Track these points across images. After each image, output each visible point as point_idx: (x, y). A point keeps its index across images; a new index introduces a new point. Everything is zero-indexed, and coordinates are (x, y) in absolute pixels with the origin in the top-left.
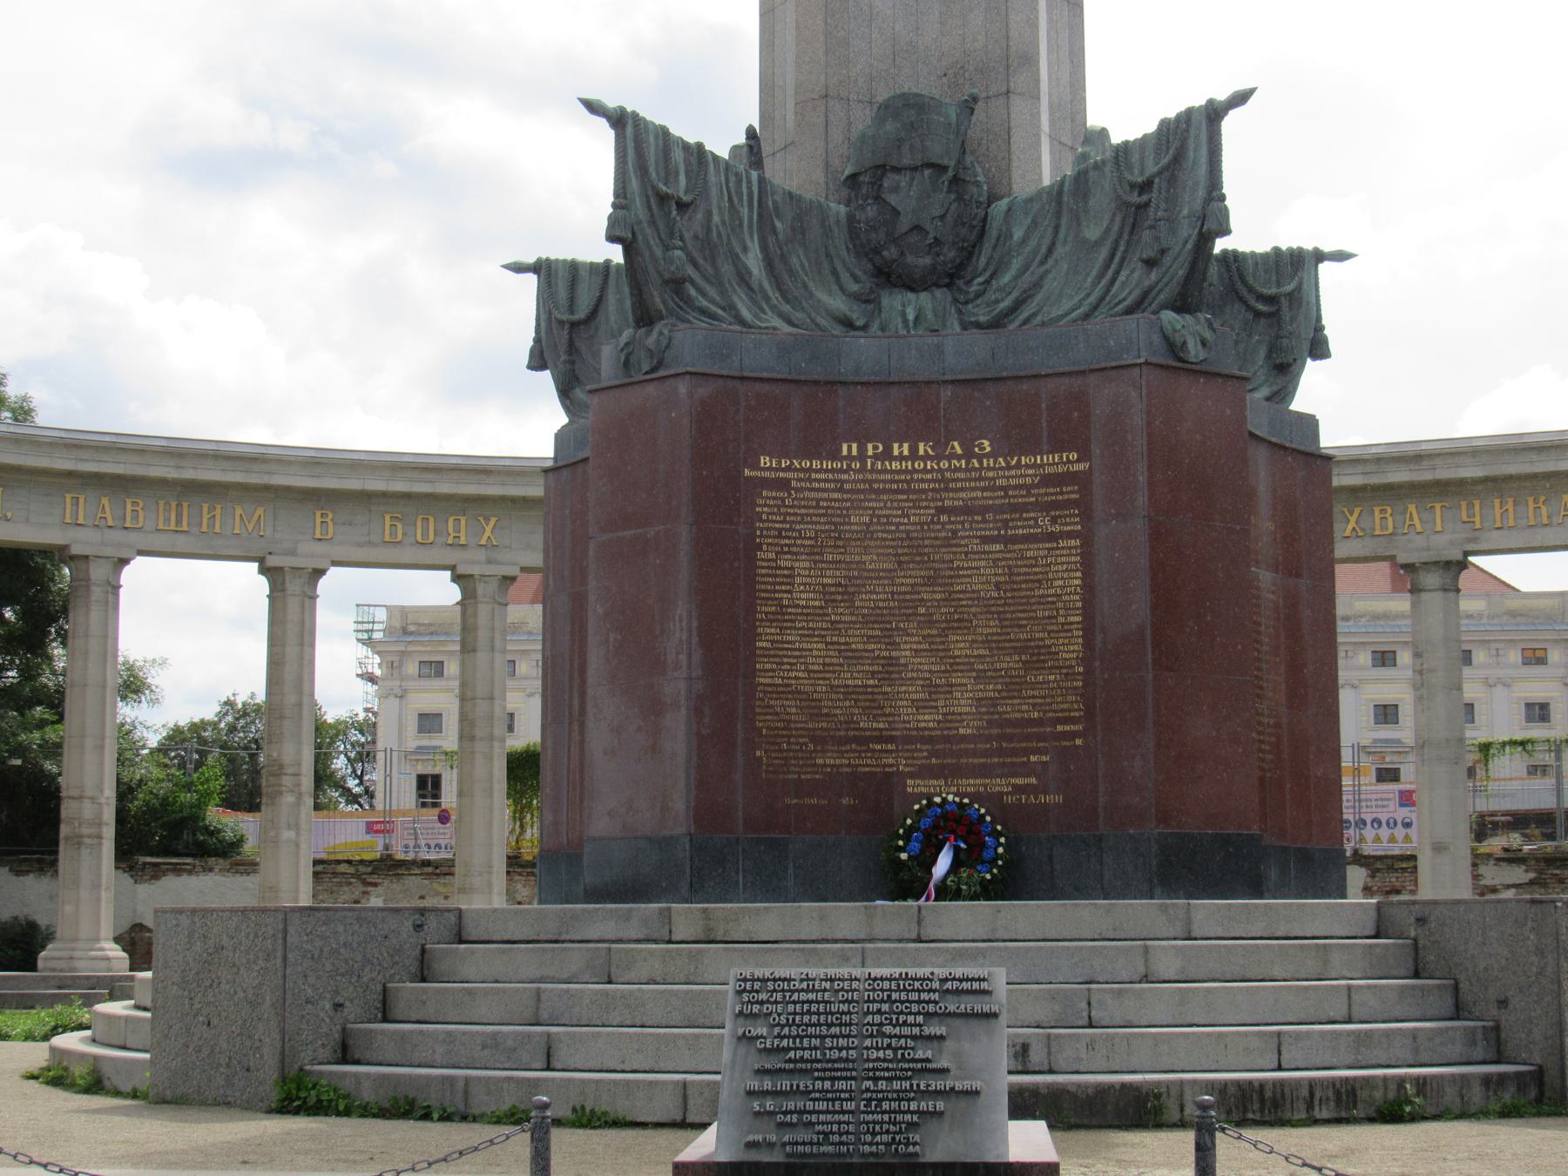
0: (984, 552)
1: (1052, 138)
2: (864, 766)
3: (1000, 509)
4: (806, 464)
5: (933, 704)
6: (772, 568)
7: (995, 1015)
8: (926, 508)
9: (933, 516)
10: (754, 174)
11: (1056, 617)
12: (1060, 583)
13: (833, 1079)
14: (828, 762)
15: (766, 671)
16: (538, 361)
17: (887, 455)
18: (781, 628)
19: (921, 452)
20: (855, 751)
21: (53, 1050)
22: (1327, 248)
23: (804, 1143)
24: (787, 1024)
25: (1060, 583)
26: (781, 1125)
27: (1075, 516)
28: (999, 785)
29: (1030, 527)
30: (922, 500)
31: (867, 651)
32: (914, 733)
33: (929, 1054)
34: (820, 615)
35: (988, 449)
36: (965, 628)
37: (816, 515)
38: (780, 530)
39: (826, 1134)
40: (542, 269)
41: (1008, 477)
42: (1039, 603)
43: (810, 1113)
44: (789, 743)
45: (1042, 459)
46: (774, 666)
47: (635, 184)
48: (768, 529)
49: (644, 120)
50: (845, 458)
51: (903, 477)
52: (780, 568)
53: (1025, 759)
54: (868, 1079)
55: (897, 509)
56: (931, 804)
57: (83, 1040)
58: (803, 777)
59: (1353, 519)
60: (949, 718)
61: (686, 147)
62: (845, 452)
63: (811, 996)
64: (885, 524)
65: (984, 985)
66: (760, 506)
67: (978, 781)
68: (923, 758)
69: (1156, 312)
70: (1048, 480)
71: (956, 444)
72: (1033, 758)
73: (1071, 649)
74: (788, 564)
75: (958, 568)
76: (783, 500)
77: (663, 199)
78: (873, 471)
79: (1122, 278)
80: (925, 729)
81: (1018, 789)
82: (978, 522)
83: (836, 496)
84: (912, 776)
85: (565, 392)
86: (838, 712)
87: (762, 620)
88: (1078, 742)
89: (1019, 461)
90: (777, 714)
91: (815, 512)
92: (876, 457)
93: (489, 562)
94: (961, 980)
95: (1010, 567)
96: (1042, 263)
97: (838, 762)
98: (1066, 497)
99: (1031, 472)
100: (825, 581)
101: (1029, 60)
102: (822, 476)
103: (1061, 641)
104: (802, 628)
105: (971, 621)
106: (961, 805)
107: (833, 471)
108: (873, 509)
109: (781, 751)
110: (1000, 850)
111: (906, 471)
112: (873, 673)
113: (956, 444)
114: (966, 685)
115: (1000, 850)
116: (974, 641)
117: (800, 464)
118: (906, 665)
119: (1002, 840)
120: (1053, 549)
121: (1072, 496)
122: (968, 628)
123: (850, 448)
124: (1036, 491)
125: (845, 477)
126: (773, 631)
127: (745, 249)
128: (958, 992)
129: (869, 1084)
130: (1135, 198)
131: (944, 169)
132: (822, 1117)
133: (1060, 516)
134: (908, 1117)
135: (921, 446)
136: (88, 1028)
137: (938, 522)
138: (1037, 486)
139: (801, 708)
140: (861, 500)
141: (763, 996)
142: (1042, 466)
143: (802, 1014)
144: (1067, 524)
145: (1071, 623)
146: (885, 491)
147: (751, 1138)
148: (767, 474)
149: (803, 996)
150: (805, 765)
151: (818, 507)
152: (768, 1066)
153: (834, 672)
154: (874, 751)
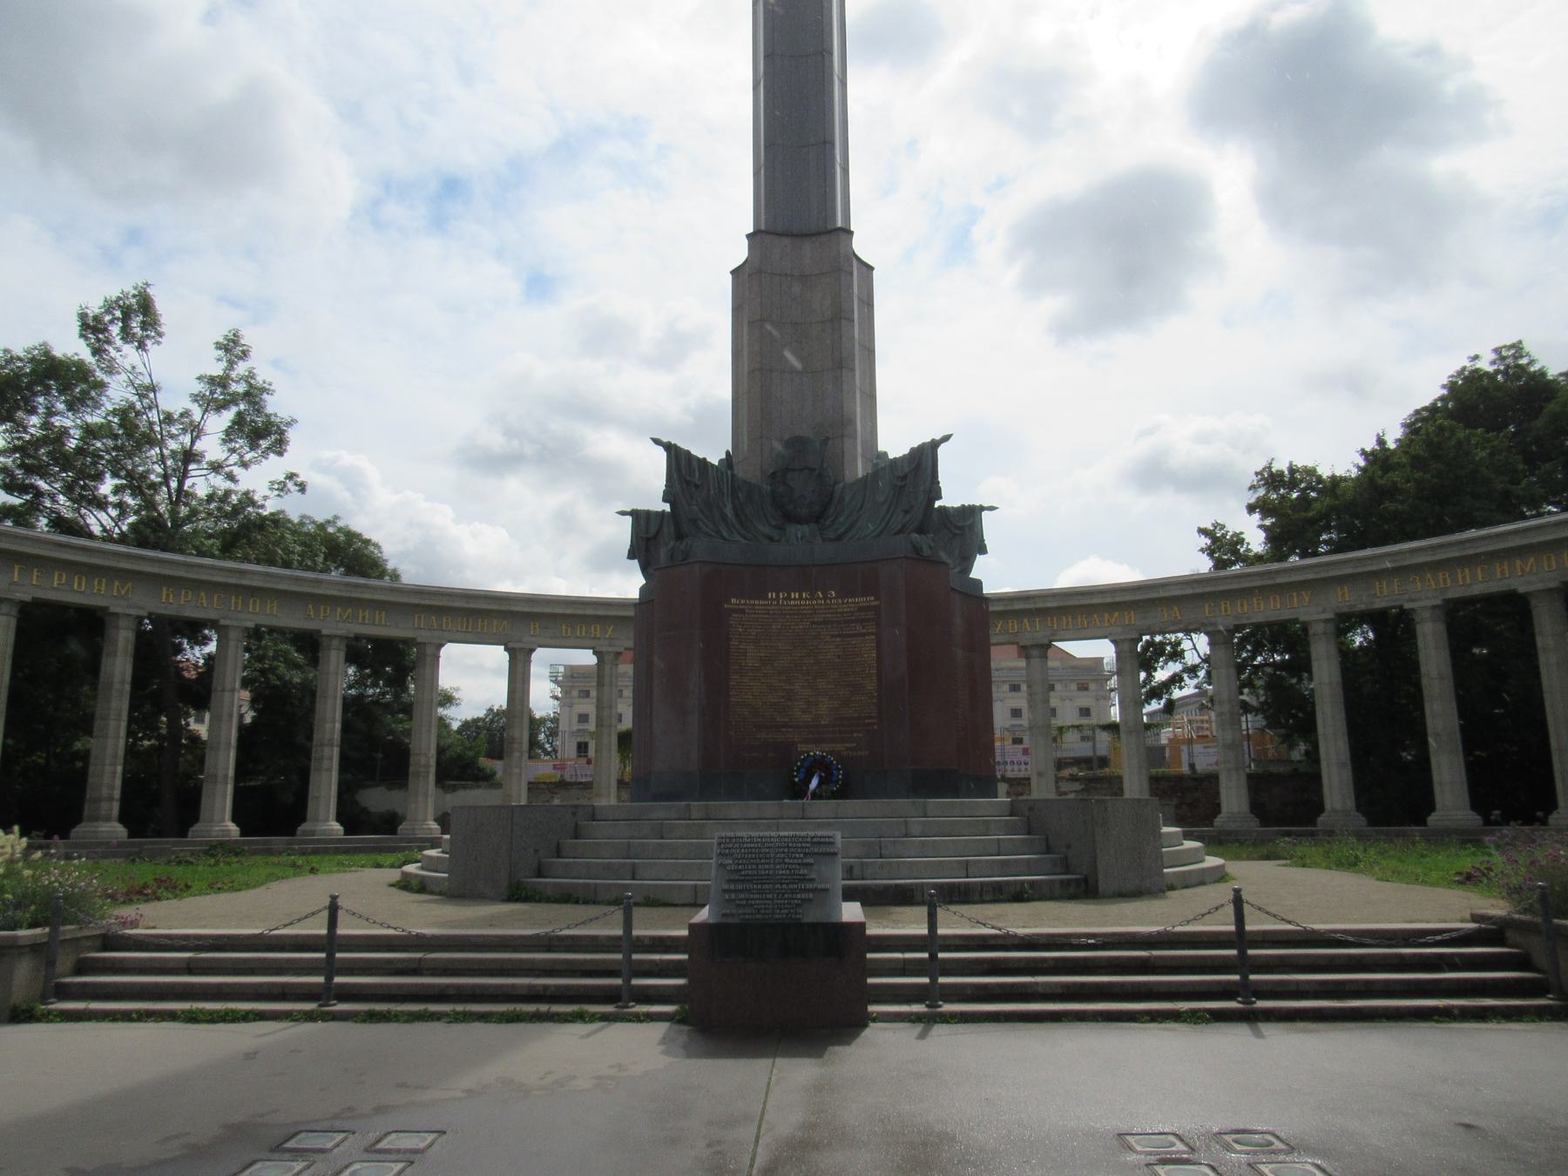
1: (863, 456)
4: (752, 602)
7: (835, 854)
10: (729, 472)
13: (762, 884)
16: (631, 555)
17: (789, 598)
19: (804, 596)
21: (405, 874)
22: (986, 506)
23: (749, 914)
24: (743, 859)
26: (738, 906)
28: (839, 747)
33: (806, 872)
39: (759, 910)
40: (635, 514)
43: (752, 899)
47: (675, 476)
49: (679, 447)
54: (778, 883)
56: (808, 755)
57: (417, 868)
59: (999, 626)
61: (699, 460)
63: (752, 845)
65: (831, 840)
69: (909, 534)
70: (861, 609)
71: (820, 593)
72: (855, 735)
73: (871, 686)
77: (688, 483)
79: (893, 519)
81: (848, 749)
83: (766, 616)
85: (644, 569)
88: (876, 727)
93: (610, 645)
94: (821, 837)
96: (858, 512)
101: (852, 422)
102: (758, 607)
106: (823, 756)
107: (764, 605)
110: (840, 777)
115: (840, 777)
119: (841, 772)
125: (769, 608)
127: (725, 505)
128: (820, 843)
129: (778, 886)
130: (899, 483)
131: (814, 470)
132: (757, 902)
134: (796, 901)
136: (419, 862)
141: (730, 845)
143: (748, 853)
147: (724, 911)
148: (734, 607)
149: (749, 845)
152: (732, 878)
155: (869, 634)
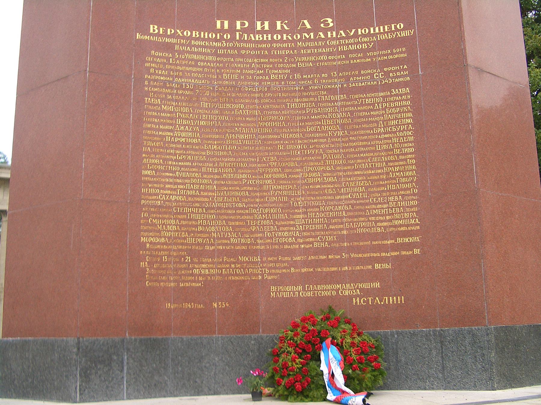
0: (331, 101)
3: (342, 68)
4: (188, 33)
5: (292, 222)
6: (157, 111)
8: (284, 68)
9: (288, 74)
11: (392, 150)
12: (395, 122)
15: (151, 195)
17: (252, 30)
18: (164, 160)
19: (279, 28)
20: (227, 263)
25: (395, 122)
27: (405, 70)
29: (367, 80)
30: (280, 63)
31: (237, 180)
32: (277, 247)
34: (196, 150)
35: (331, 25)
36: (317, 161)
37: (195, 72)
38: (165, 82)
41: (348, 45)
42: (378, 139)
44: (169, 256)
45: (374, 30)
46: (158, 191)
48: (155, 80)
50: (220, 31)
51: (264, 46)
52: (164, 111)
53: (370, 267)
55: (259, 69)
60: (305, 234)
62: (219, 26)
64: (250, 80)
66: (148, 62)
67: (329, 287)
68: (285, 268)
71: (306, 22)
72: (377, 266)
74: (171, 108)
75: (310, 114)
76: (168, 59)
78: (240, 41)
80: (285, 243)
81: (366, 293)
82: (325, 78)
83: (210, 58)
84: (275, 283)
86: (213, 229)
87: (147, 153)
88: (417, 251)
89: (356, 32)
90: (159, 231)
91: (194, 69)
92: (243, 30)
95: (352, 112)
98: (396, 56)
99: (365, 39)
100: (202, 123)
103: (397, 169)
104: (182, 161)
105: (321, 155)
107: (209, 40)
108: (242, 69)
111: (267, 42)
112: (241, 197)
113: (306, 22)
114: (318, 207)
116: (324, 171)
117: (183, 33)
118: (268, 191)
120: (387, 96)
121: (402, 55)
122: (319, 161)
123: (222, 24)
124: (371, 54)
126: (156, 161)
133: (391, 71)
135: (279, 23)
137: (293, 80)
138: (373, 49)
139: (181, 226)
140: (232, 62)
142: (375, 35)
144: (397, 77)
145: (406, 154)
146: (252, 57)
148: (155, 39)
151: (196, 66)
153: (208, 197)
154: (244, 262)
155: (398, 85)
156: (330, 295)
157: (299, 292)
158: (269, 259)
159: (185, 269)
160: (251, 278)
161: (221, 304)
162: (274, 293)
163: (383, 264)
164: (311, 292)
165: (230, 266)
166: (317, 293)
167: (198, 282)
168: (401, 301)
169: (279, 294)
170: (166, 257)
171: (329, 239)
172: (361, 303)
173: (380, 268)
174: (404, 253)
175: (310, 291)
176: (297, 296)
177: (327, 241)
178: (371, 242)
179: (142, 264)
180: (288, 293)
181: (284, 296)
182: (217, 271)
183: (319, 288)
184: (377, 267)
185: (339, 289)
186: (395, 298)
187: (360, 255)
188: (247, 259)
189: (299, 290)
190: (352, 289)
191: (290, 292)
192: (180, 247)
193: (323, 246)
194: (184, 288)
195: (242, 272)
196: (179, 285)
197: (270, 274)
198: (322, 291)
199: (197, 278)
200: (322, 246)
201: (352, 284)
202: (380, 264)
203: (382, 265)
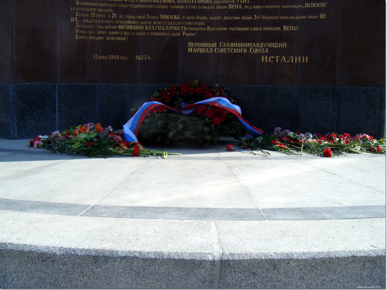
2: (155, 31)
14: (128, 28)
20: (149, 20)
32: (194, 7)
44: (97, 13)
53: (279, 29)
58: (108, 38)
67: (241, 45)
68: (201, 26)
72: (285, 28)
81: (273, 52)
84: (193, 39)
88: (323, 16)
97: (136, 28)
109: (90, 18)
150: (111, 30)
154: (164, 20)
156: (241, 52)
157: (214, 48)
158: (188, 18)
159: (111, 24)
160: (171, 34)
161: (143, 57)
162: (191, 48)
163: (291, 27)
164: (225, 49)
165: (152, 22)
166: (230, 50)
167: (123, 36)
168: (305, 60)
169: (196, 50)
170: (94, 13)
171: (243, 2)
172: (269, 60)
173: (288, 30)
174: (310, 17)
175: (224, 48)
176: (212, 52)
177: (241, 4)
178: (281, 6)
179: (72, 20)
180: (204, 49)
181: (200, 52)
182: (141, 28)
183: (232, 46)
184: (285, 29)
185: (250, 47)
186: (300, 58)
187: (270, 18)
188: (168, 17)
189: (214, 47)
190: (261, 48)
191: (205, 48)
192: (107, 5)
193: (237, 8)
194: (111, 41)
195: (163, 29)
196: (105, 38)
197: (187, 31)
198: (234, 49)
199: (121, 32)
200: (236, 7)
201: (262, 43)
202: (288, 27)
203: (290, 27)
